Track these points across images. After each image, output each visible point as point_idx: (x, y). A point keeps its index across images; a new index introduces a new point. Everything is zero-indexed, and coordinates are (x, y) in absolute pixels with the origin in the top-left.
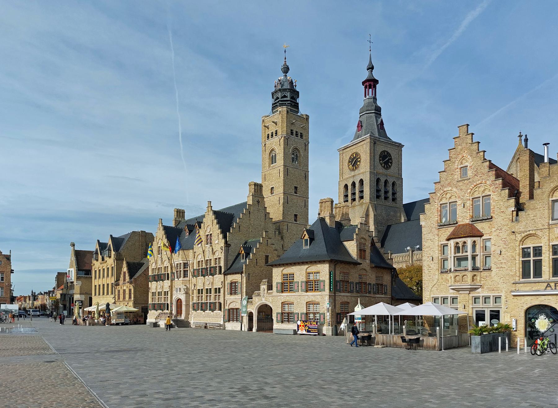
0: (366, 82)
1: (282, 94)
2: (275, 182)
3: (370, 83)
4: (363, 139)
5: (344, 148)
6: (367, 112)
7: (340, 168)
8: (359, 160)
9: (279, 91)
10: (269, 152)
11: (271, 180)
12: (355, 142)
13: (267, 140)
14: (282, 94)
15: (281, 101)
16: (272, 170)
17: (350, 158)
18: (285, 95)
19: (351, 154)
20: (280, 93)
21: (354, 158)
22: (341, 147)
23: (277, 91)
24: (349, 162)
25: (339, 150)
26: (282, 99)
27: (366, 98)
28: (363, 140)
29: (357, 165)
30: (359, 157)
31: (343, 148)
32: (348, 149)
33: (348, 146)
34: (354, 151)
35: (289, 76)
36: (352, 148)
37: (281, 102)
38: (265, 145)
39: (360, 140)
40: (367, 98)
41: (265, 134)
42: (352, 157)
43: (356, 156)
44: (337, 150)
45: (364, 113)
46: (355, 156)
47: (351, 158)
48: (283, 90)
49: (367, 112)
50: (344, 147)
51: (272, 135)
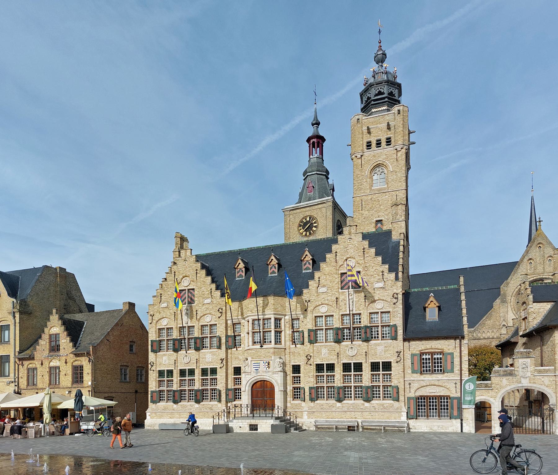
0: (314, 138)
1: (389, 89)
2: (386, 213)
3: (319, 140)
4: (323, 201)
5: (292, 209)
6: (318, 172)
7: (285, 231)
8: (314, 225)
9: (385, 82)
10: (371, 168)
11: (375, 210)
12: (310, 203)
13: (366, 150)
14: (376, 91)
15: (374, 100)
16: (380, 195)
17: (302, 221)
18: (380, 91)
19: (302, 217)
20: (386, 86)
21: (307, 222)
22: (286, 207)
23: (382, 83)
24: (300, 226)
25: (284, 211)
26: (376, 98)
27: (313, 157)
28: (322, 202)
29: (312, 231)
30: (315, 222)
31: (291, 208)
32: (298, 211)
33: (299, 207)
34: (308, 213)
35: (387, 70)
36: (304, 209)
37: (374, 101)
38: (361, 156)
39: (318, 202)
40: (315, 156)
41: (363, 141)
42: (305, 221)
43: (310, 220)
44: (282, 210)
45: (313, 173)
46: (308, 219)
47: (303, 221)
48: (391, 83)
49: (318, 172)
50: (293, 207)
51: (379, 144)
